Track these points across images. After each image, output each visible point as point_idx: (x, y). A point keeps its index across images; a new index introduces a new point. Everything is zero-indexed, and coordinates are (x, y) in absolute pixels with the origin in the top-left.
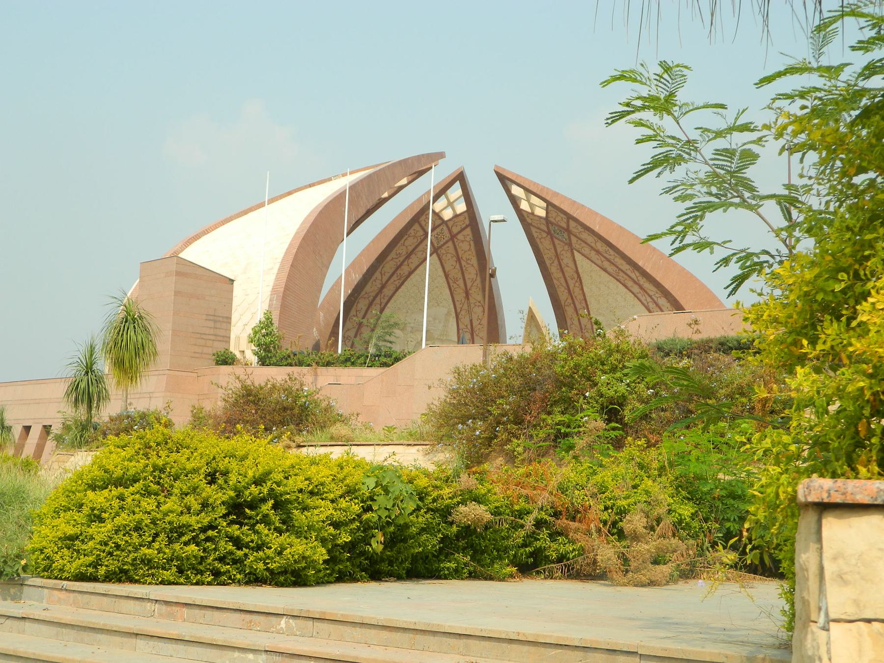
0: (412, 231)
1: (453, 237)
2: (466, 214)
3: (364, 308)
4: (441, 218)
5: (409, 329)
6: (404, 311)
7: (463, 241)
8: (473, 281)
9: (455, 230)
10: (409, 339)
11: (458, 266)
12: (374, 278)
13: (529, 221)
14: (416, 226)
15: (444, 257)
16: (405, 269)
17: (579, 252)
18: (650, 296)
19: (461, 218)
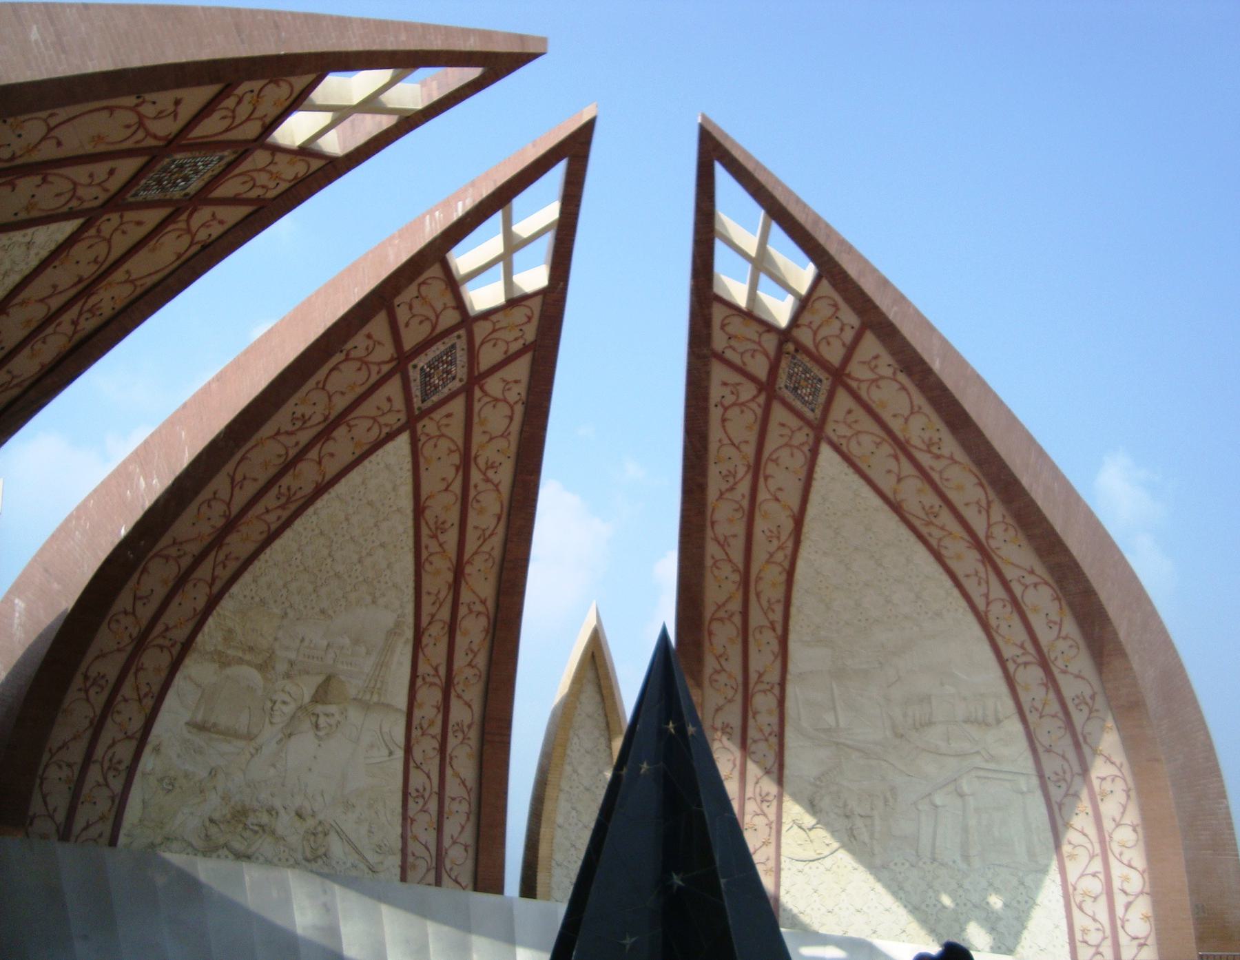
0: (359, 342)
1: (475, 379)
2: (536, 304)
3: (161, 592)
4: (460, 304)
5: (281, 667)
6: (277, 611)
7: (496, 400)
8: (484, 539)
9: (489, 356)
10: (279, 697)
11: (457, 487)
12: (206, 494)
13: (719, 341)
14: (378, 326)
15: (427, 450)
16: (307, 476)
17: (837, 448)
18: (1005, 584)
19: (519, 314)
